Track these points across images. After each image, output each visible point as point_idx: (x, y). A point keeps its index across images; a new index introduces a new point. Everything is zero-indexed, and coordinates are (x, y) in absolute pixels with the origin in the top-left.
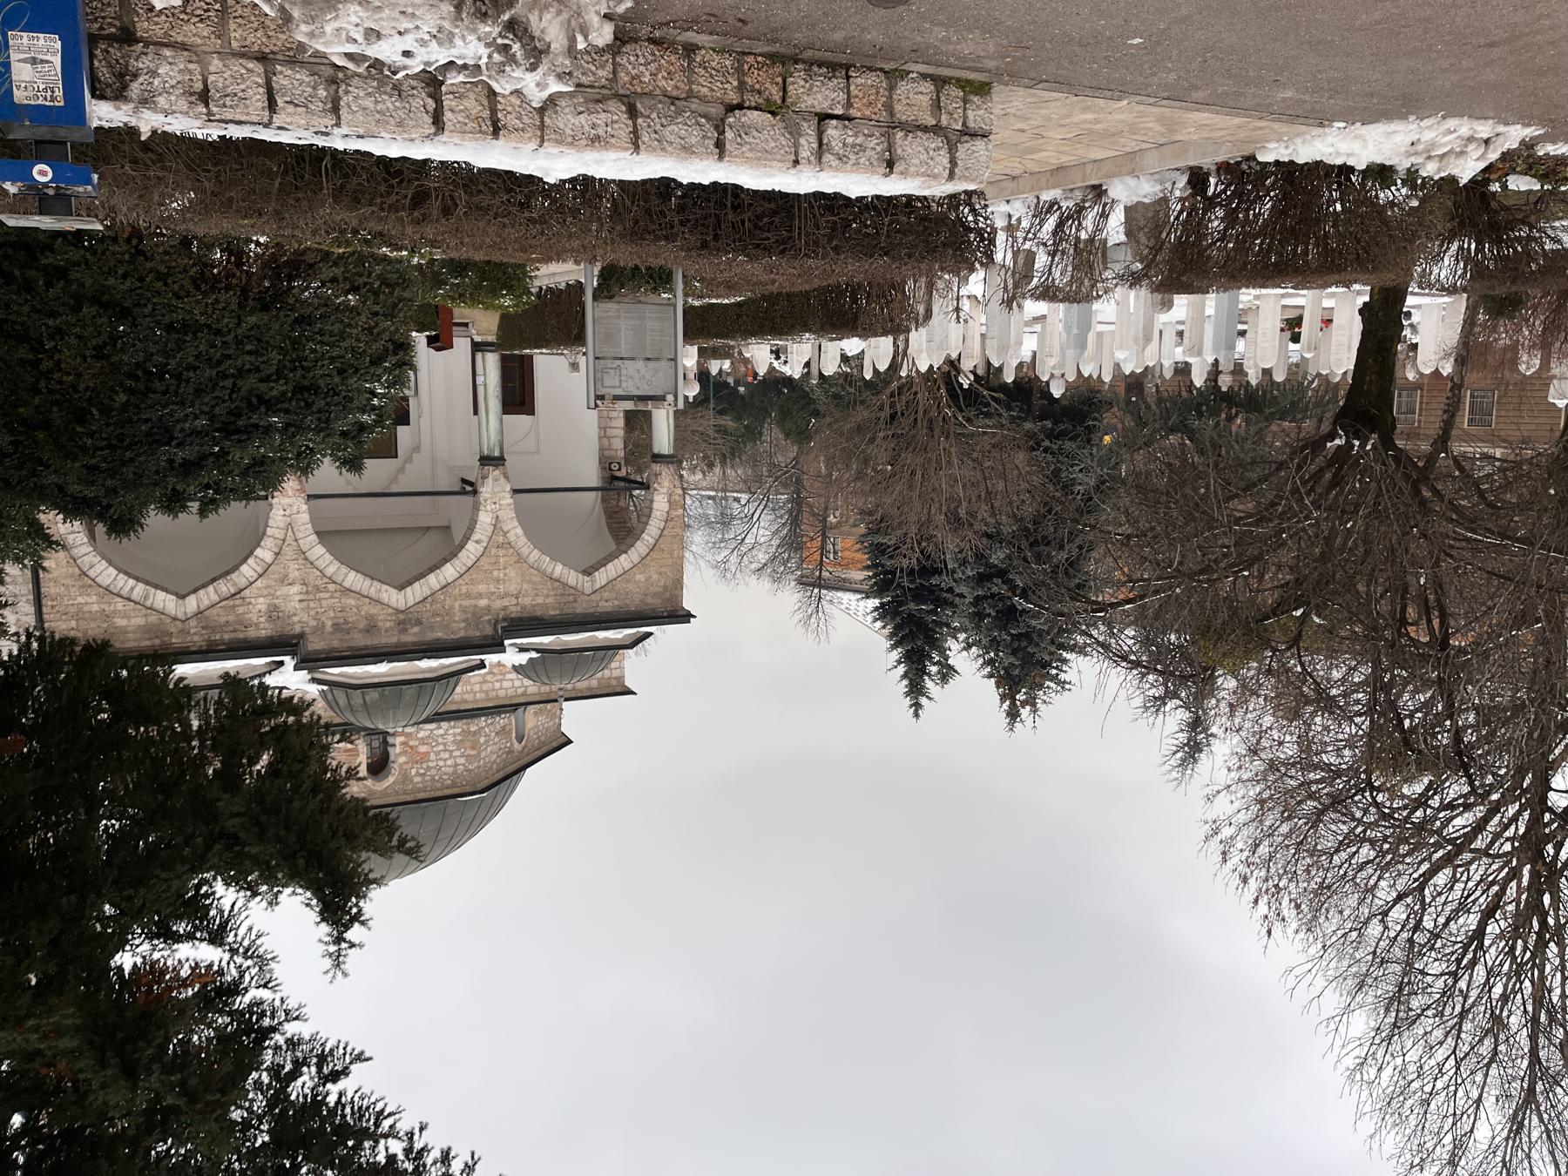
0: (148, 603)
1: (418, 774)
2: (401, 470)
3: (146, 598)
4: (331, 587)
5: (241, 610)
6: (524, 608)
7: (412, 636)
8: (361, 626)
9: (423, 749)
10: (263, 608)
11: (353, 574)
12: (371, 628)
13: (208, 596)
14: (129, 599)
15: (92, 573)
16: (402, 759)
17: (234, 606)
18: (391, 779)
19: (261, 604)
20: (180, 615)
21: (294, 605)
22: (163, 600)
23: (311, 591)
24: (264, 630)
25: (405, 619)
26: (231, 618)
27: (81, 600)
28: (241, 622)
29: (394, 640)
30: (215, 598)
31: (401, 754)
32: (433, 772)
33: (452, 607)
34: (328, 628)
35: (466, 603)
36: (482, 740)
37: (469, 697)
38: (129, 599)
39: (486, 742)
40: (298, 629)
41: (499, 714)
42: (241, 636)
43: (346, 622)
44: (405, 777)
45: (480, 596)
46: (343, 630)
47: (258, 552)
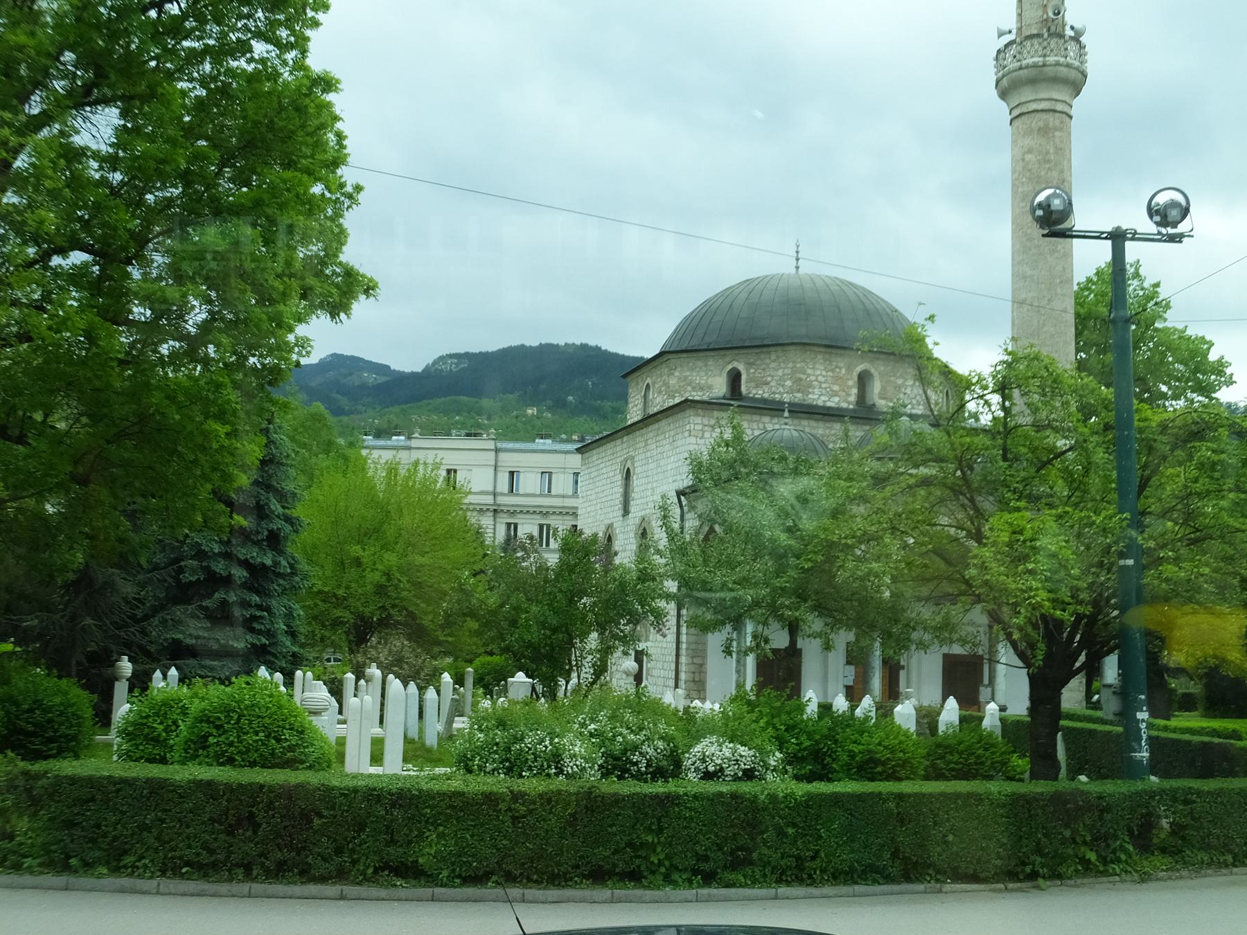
1: (840, 369)
9: (836, 388)
18: (859, 369)
31: (851, 387)
39: (782, 379)
44: (850, 369)
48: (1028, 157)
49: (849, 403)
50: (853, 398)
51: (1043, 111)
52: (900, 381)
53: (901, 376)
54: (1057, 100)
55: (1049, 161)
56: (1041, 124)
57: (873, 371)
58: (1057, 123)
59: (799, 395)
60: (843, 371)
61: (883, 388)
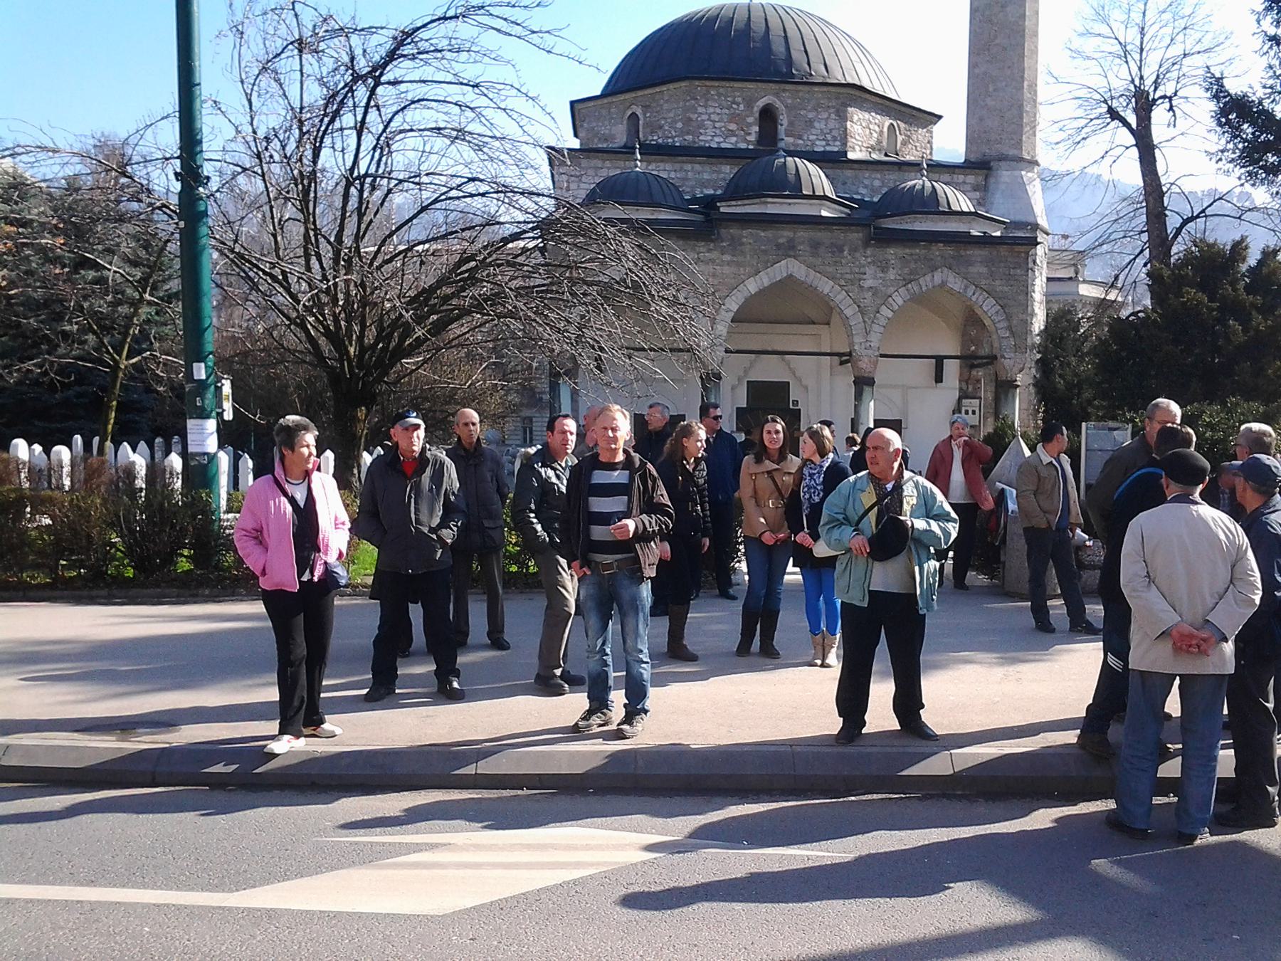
1: (738, 104)
2: (746, 372)
3: (966, 287)
6: (693, 249)
7: (785, 234)
9: (733, 127)
12: (815, 246)
16: (750, 120)
18: (761, 103)
19: (892, 275)
21: (870, 271)
24: (892, 252)
25: (789, 250)
26: (913, 266)
27: (1006, 289)
31: (750, 125)
33: (752, 257)
35: (740, 259)
37: (697, 167)
41: (658, 146)
42: (907, 251)
43: (833, 253)
44: (749, 103)
45: (729, 263)
49: (749, 142)
50: (752, 138)
57: (778, 104)
59: (689, 138)
61: (791, 124)
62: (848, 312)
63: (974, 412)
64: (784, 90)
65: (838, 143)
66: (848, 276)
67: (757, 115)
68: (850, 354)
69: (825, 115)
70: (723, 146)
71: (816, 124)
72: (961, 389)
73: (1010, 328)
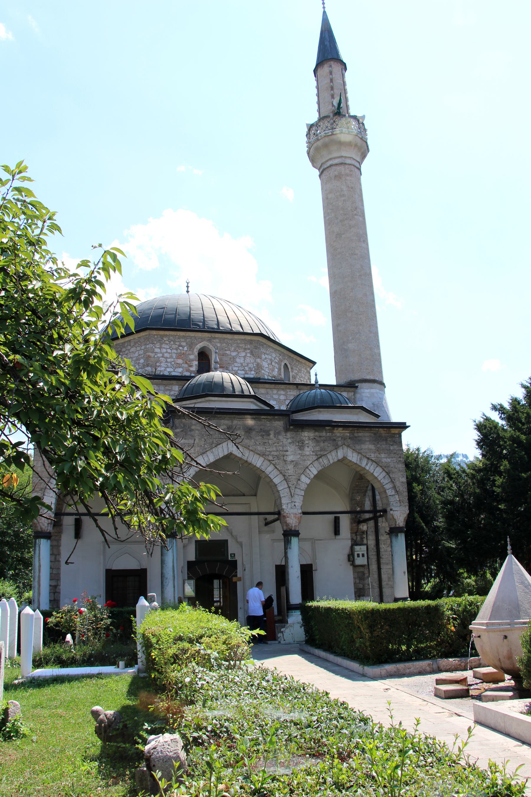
0: (360, 456)
1: (183, 347)
3: (361, 459)
4: (271, 458)
5: (318, 448)
8: (254, 433)
9: (180, 361)
10: (306, 449)
11: (258, 465)
13: (334, 457)
14: (368, 459)
15: (384, 474)
16: (192, 357)
17: (321, 451)
18: (199, 346)
19: (307, 451)
20: (345, 448)
22: (353, 457)
23: (281, 456)
24: (307, 435)
26: (322, 444)
27: (389, 460)
28: (317, 442)
29: (235, 422)
30: (329, 456)
32: (174, 346)
33: (200, 439)
34: (272, 433)
36: (142, 361)
38: (368, 459)
40: (289, 434)
42: (317, 434)
43: (262, 436)
44: (191, 346)
46: (264, 431)
47: (308, 481)
48: (330, 196)
49: (191, 372)
51: (336, 165)
52: (234, 354)
53: (235, 350)
54: (346, 157)
55: (343, 195)
56: (336, 173)
57: (211, 347)
58: (348, 171)
60: (186, 349)
62: (276, 481)
63: (363, 555)
64: (215, 338)
65: (253, 372)
66: (275, 453)
67: (196, 353)
68: (279, 513)
69: (243, 354)
70: (174, 374)
71: (238, 360)
72: (352, 539)
73: (394, 487)
